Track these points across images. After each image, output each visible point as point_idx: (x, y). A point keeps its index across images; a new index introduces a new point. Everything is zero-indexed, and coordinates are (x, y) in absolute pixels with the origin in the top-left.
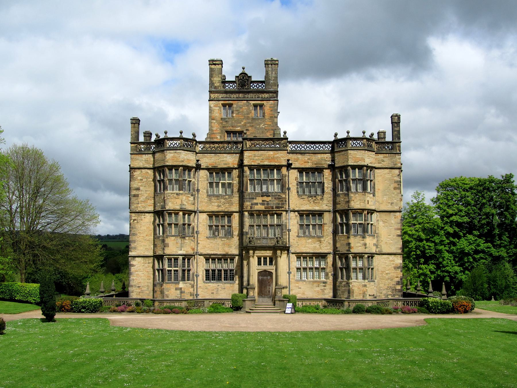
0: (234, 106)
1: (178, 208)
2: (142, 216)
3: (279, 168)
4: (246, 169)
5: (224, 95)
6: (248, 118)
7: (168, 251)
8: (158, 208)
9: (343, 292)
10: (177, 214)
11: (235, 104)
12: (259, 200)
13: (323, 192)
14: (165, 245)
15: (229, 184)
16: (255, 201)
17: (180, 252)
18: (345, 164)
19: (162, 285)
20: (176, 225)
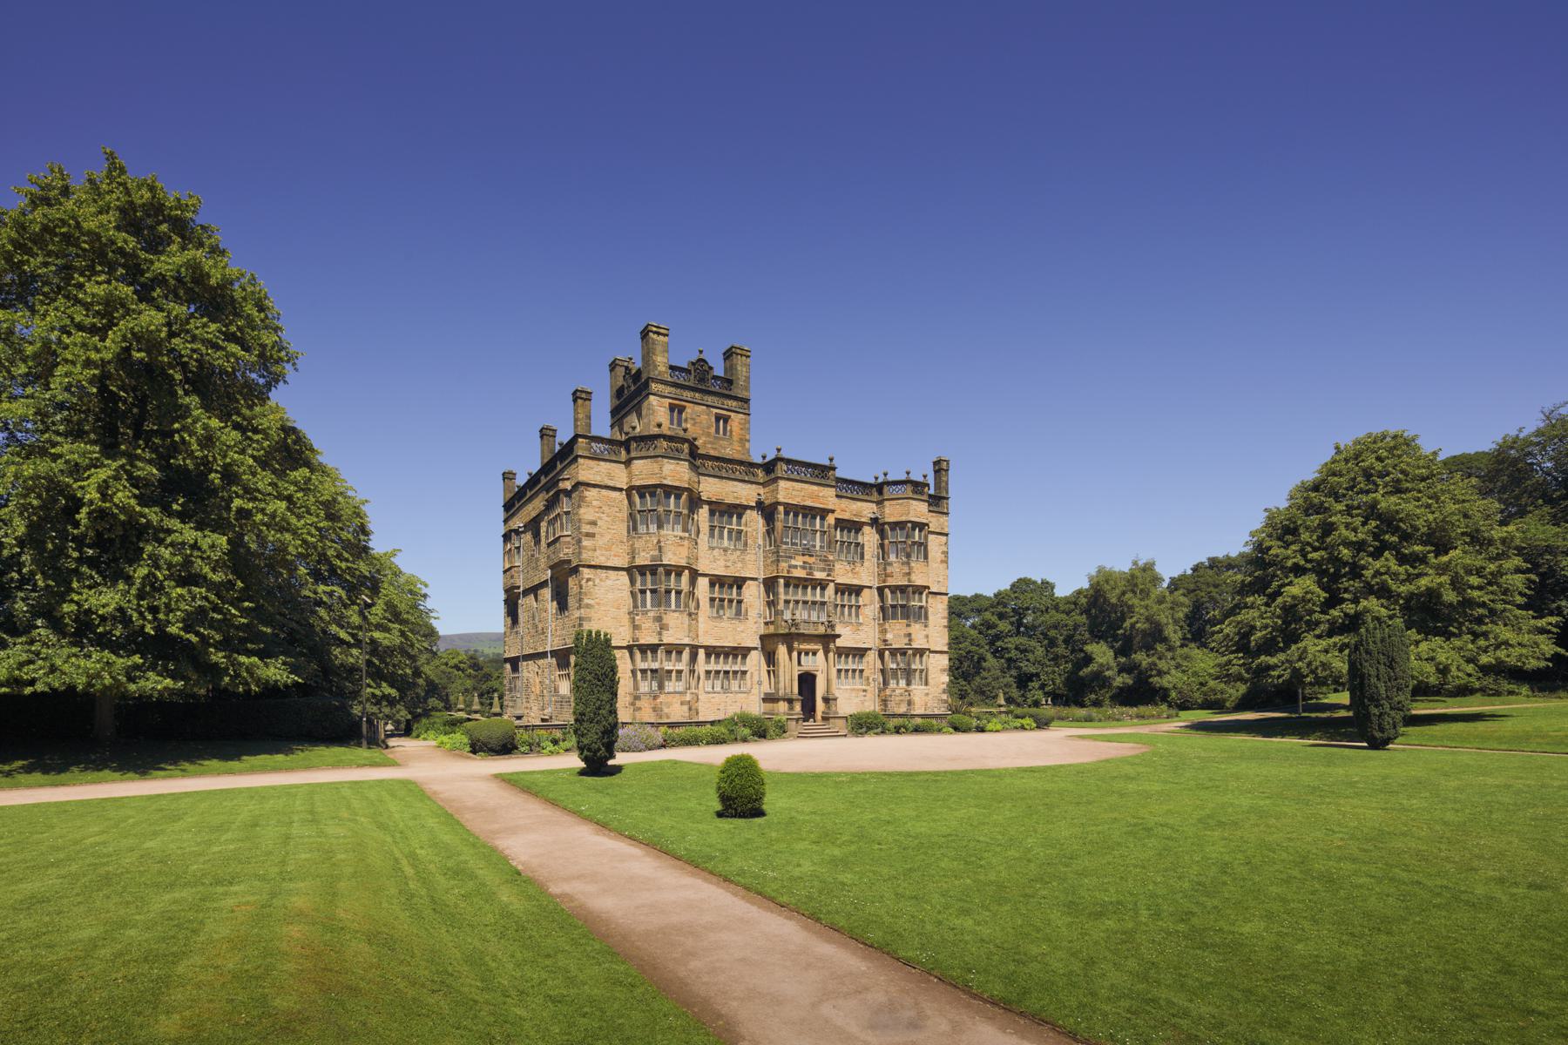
0: (688, 410)
1: (683, 563)
2: (603, 573)
3: (824, 513)
4: (781, 508)
5: (673, 390)
6: (709, 435)
7: (668, 638)
8: (643, 559)
9: (898, 704)
10: (679, 575)
11: (690, 408)
12: (798, 561)
13: (862, 557)
14: (663, 627)
15: (740, 532)
16: (793, 562)
17: (686, 641)
18: (904, 519)
19: (655, 698)
20: (678, 593)
